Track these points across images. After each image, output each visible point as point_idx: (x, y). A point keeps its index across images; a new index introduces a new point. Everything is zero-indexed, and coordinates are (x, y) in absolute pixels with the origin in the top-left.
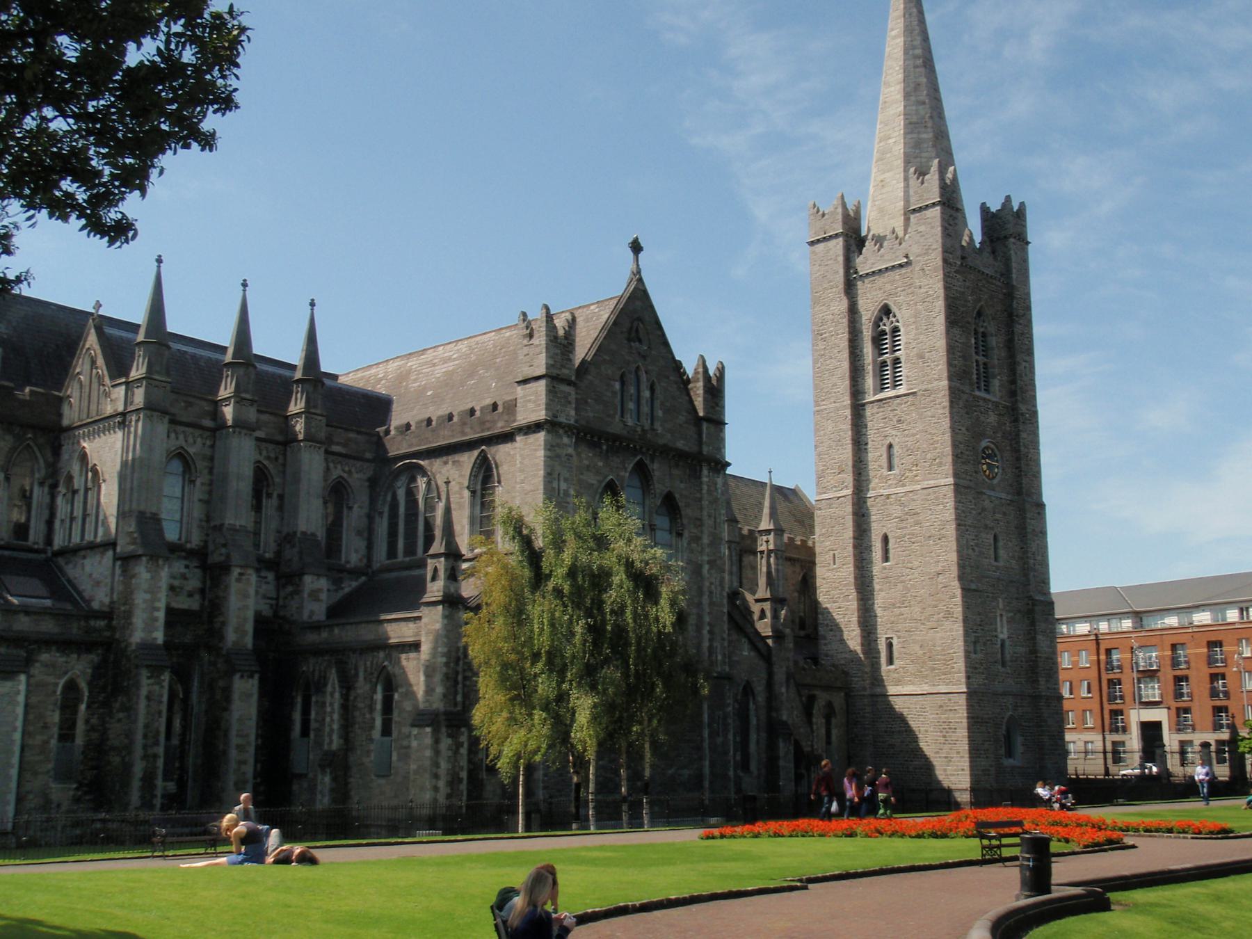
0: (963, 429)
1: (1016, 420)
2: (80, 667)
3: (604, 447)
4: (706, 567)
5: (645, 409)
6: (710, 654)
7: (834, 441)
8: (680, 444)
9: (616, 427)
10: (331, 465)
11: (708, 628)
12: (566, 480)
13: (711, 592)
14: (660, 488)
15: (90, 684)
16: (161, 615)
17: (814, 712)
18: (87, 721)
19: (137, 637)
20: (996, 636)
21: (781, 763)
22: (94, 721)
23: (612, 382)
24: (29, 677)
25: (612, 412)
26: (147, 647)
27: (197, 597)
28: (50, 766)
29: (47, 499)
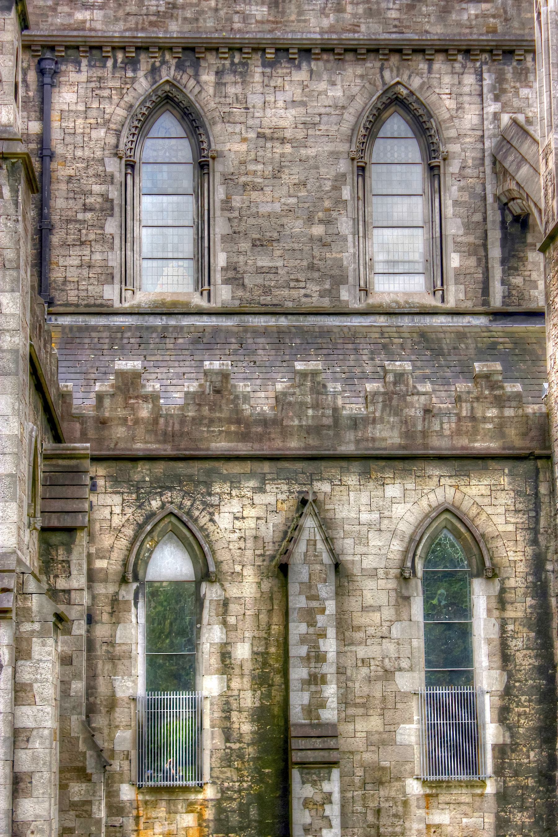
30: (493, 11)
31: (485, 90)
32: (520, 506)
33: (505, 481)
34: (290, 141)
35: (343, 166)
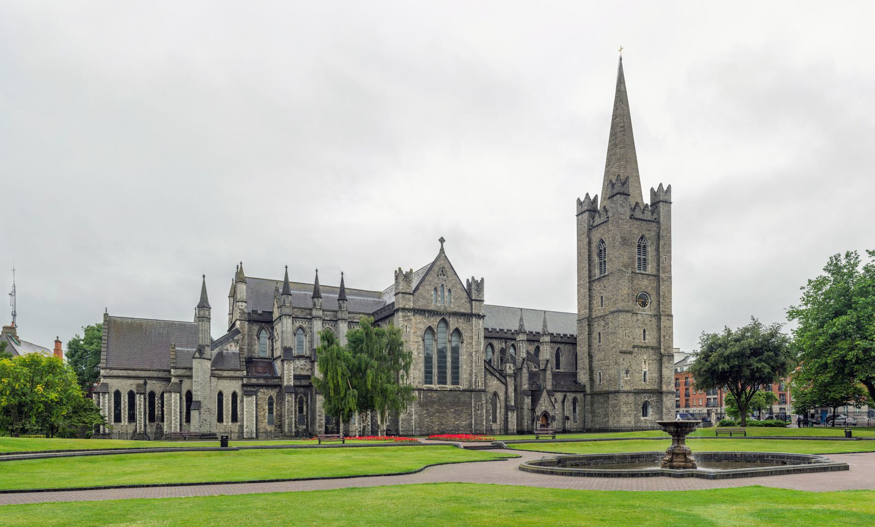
0: (627, 289)
1: (659, 282)
2: (273, 393)
3: (427, 315)
4: (474, 353)
5: (446, 299)
6: (475, 384)
8: (462, 311)
9: (432, 307)
10: (355, 326)
11: (474, 374)
12: (409, 327)
13: (476, 362)
14: (452, 327)
15: (276, 398)
16: (292, 377)
18: (276, 408)
19: (285, 384)
20: (641, 370)
21: (509, 420)
22: (278, 408)
23: (430, 292)
24: (256, 396)
25: (430, 302)
26: (288, 387)
27: (310, 371)
28: (266, 421)
29: (271, 343)
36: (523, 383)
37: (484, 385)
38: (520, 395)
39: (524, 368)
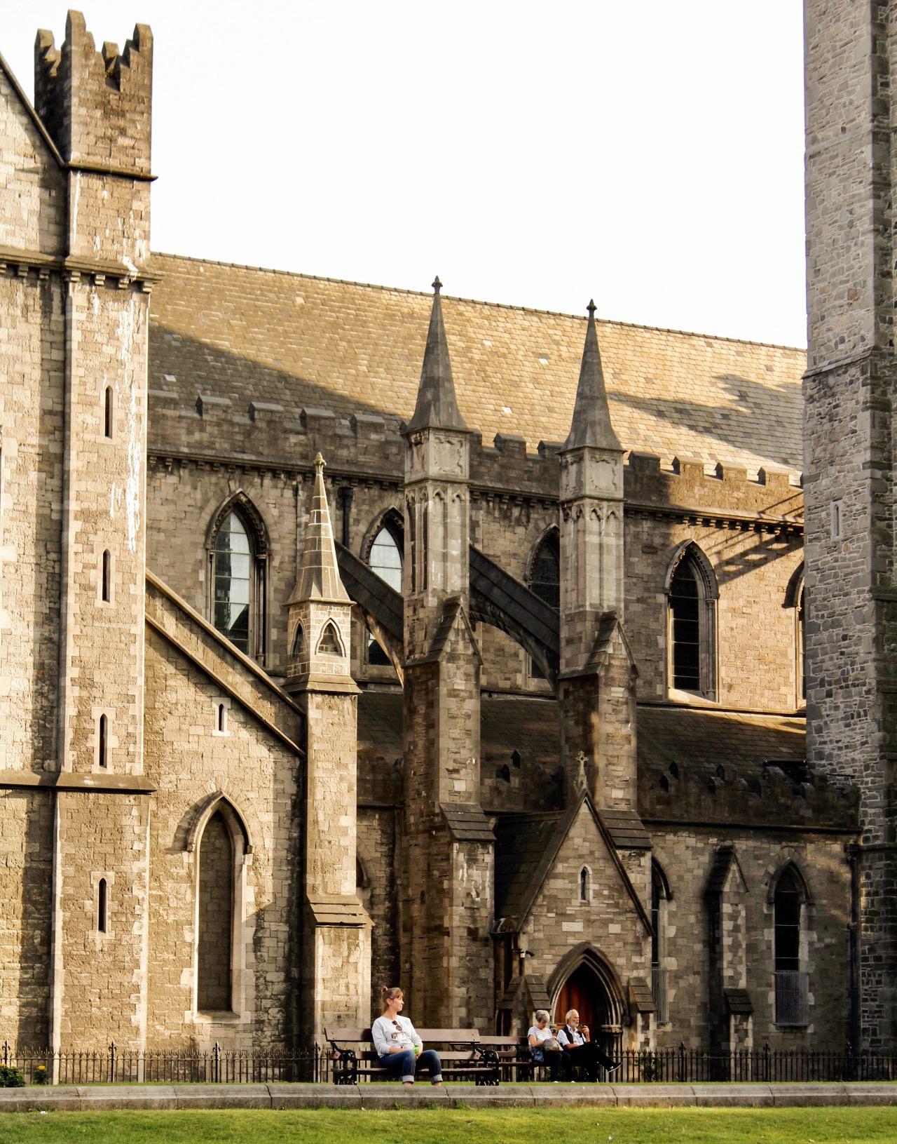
7: (841, 228)
13: (87, 588)
17: (726, 888)
30: (306, 442)
31: (299, 504)
32: (384, 841)
33: (375, 823)
34: (164, 531)
35: (200, 554)
36: (445, 763)
37: (140, 749)
38: (421, 839)
39: (453, 657)
